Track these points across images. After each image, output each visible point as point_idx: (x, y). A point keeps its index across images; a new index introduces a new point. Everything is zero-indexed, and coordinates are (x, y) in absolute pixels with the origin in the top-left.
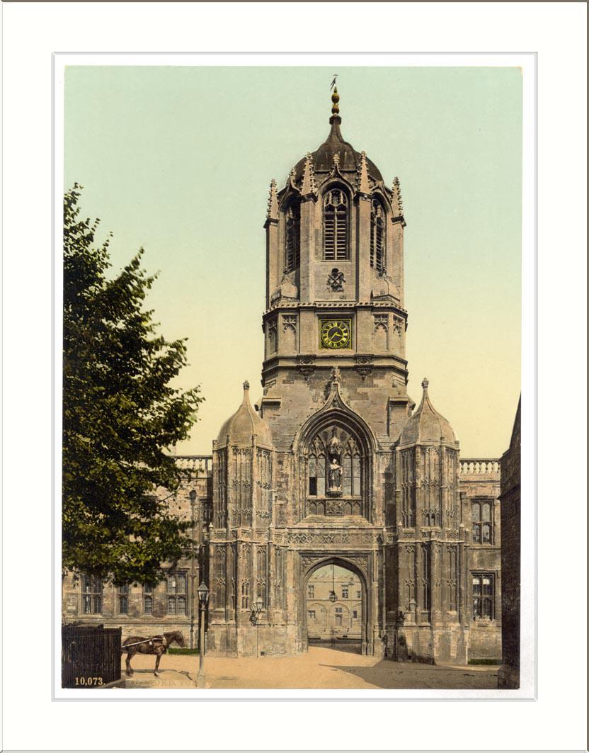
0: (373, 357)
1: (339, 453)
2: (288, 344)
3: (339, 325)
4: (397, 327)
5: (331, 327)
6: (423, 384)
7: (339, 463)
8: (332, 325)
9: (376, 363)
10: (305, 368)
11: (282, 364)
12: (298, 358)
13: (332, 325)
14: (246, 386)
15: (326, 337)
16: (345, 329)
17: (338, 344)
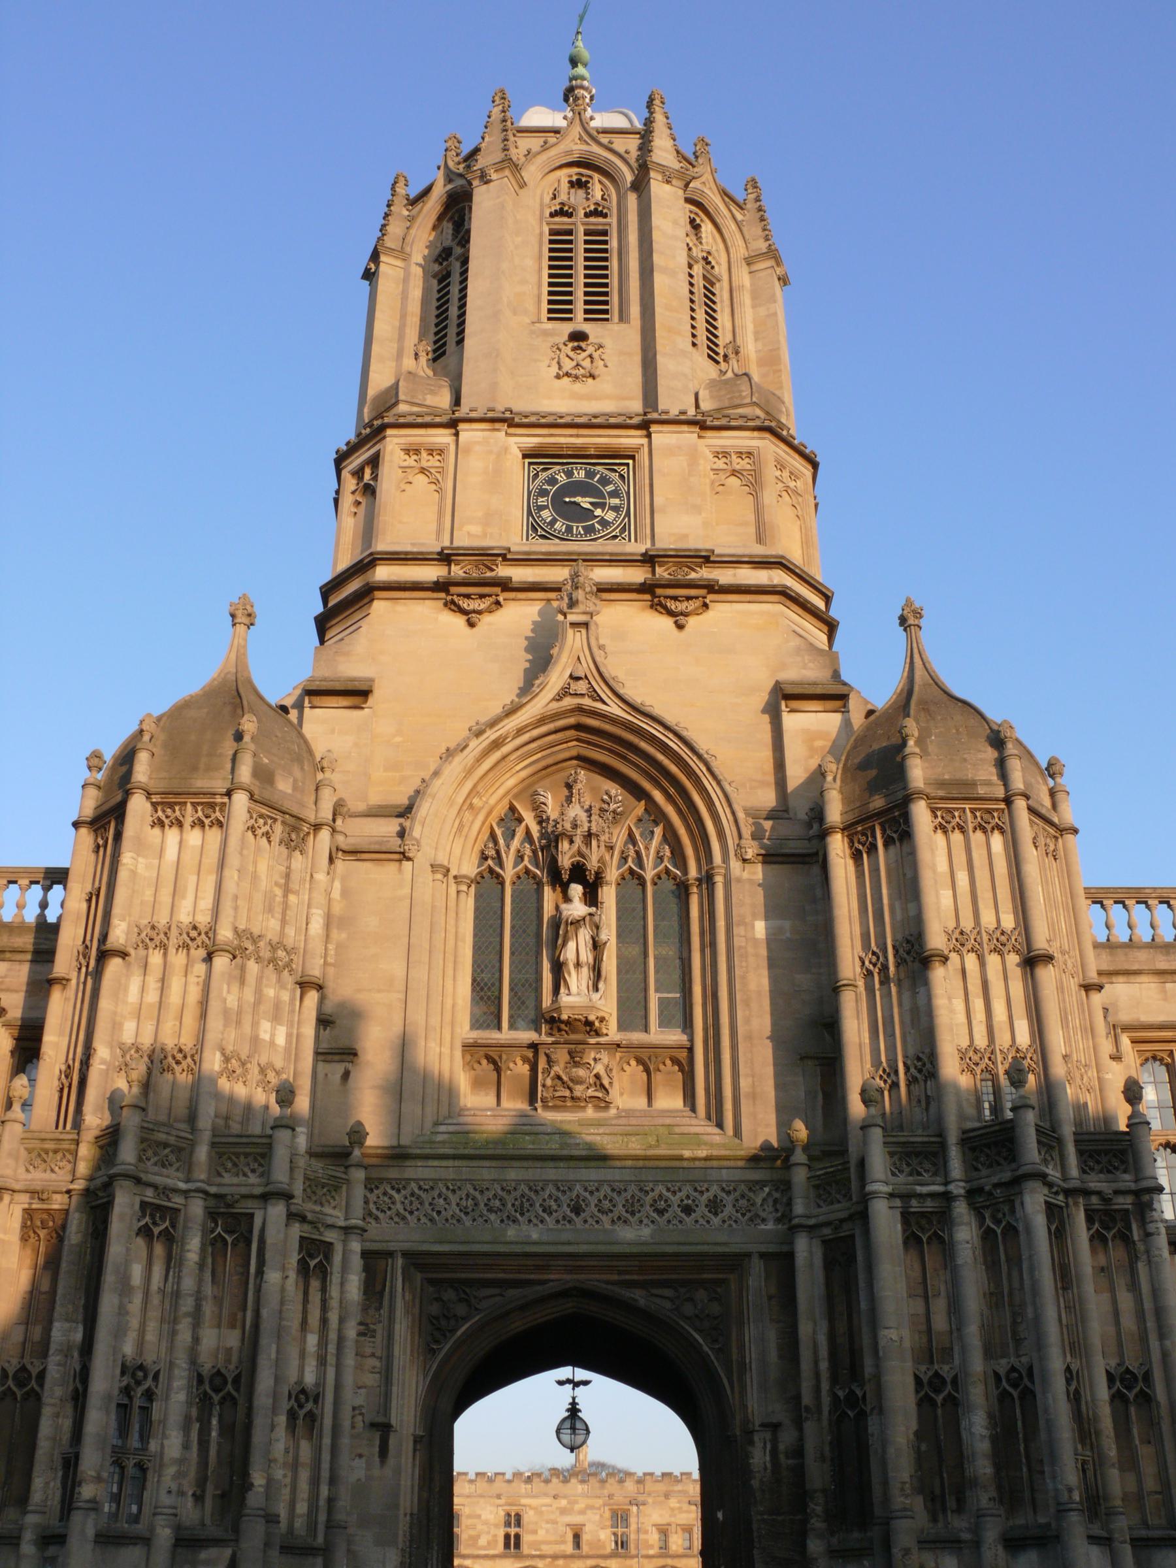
0: (706, 559)
1: (592, 864)
2: (411, 516)
3: (590, 475)
4: (787, 489)
5: (562, 478)
6: (903, 620)
7: (591, 898)
8: (569, 474)
9: (725, 576)
10: (468, 582)
11: (383, 573)
12: (445, 558)
13: (569, 474)
14: (243, 616)
15: (541, 508)
16: (610, 488)
17: (590, 530)
